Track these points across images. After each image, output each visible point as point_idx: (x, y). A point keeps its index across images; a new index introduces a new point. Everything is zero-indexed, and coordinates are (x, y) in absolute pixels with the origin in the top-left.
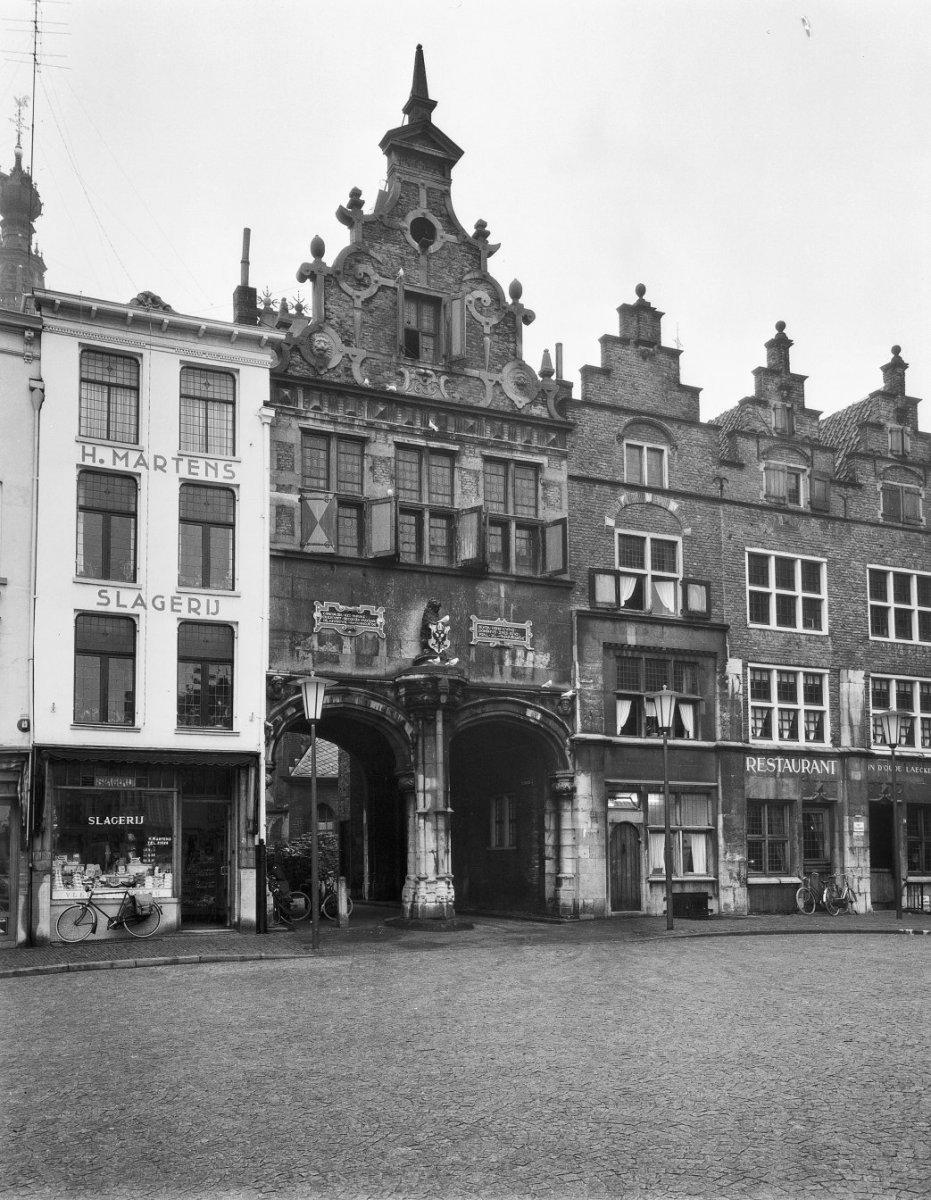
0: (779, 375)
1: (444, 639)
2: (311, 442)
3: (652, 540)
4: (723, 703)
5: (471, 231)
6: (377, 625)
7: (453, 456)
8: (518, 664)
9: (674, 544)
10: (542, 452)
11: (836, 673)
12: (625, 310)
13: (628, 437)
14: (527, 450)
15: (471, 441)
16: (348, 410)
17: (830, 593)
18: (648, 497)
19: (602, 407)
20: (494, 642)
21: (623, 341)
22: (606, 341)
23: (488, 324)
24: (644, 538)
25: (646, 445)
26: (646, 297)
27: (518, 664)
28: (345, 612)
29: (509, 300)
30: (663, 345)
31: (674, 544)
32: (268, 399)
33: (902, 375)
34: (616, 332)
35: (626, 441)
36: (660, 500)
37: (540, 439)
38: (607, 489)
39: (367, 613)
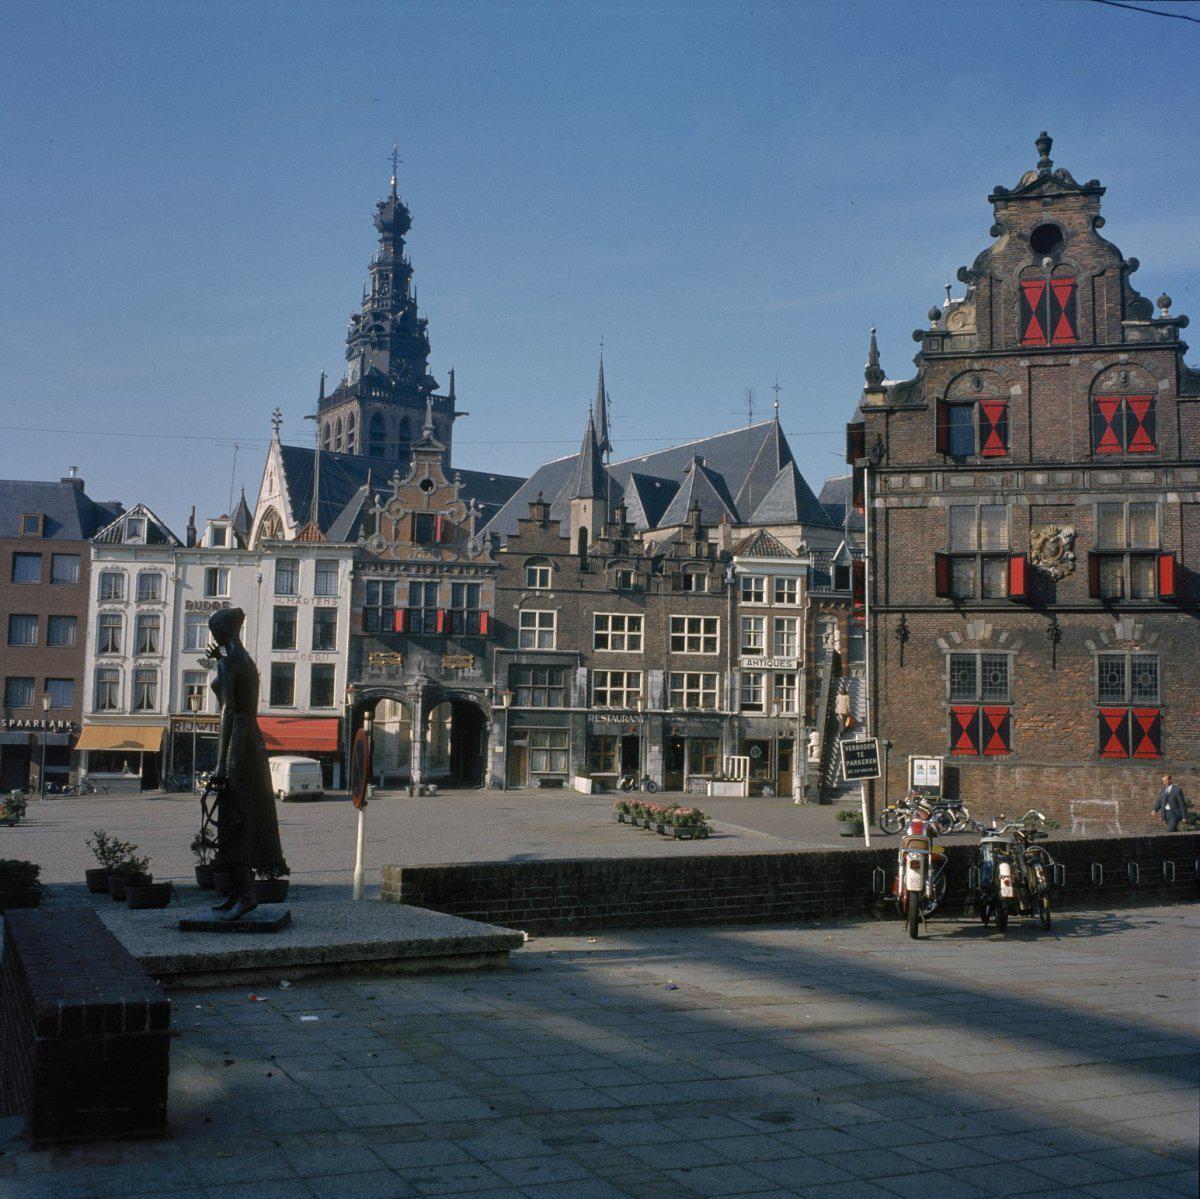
4: (575, 689)
8: (466, 674)
10: (482, 578)
11: (646, 672)
14: (473, 577)
15: (446, 577)
17: (645, 631)
27: (466, 674)
38: (516, 592)
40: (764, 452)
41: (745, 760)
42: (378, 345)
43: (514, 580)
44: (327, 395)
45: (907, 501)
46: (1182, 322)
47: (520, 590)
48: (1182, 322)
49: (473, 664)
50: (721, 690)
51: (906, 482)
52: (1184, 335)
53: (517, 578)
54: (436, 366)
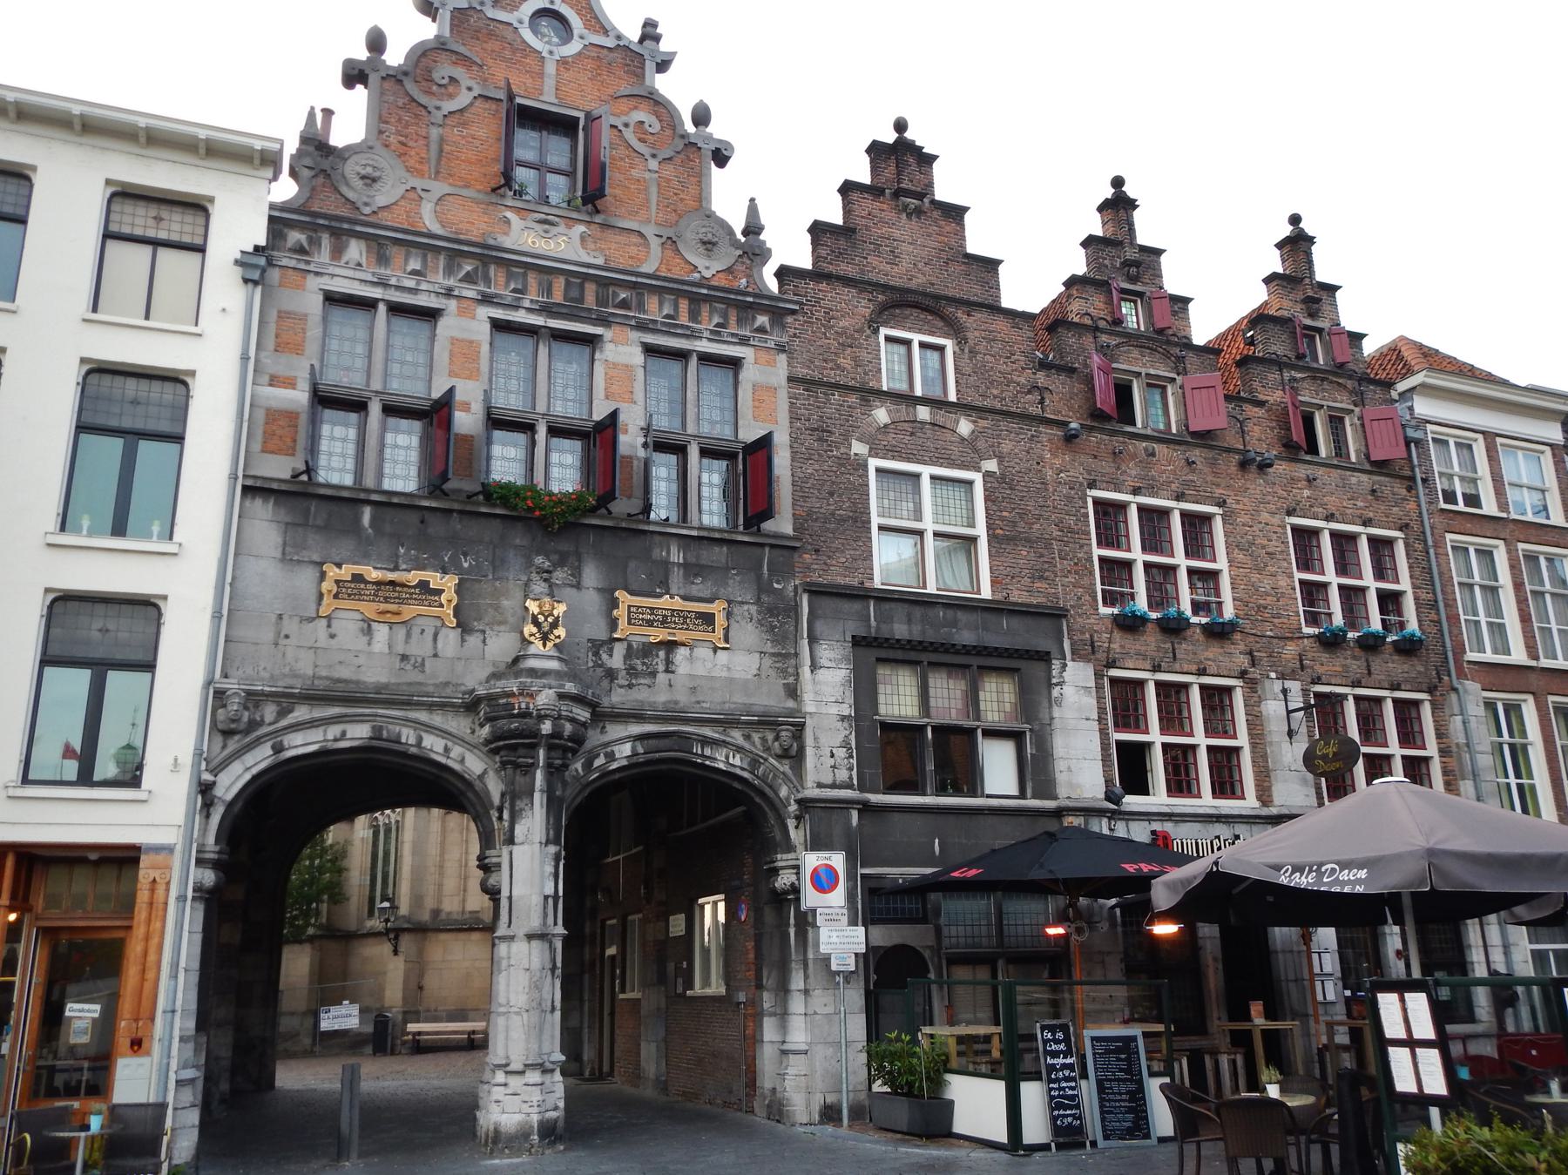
0: (1119, 256)
1: (554, 625)
2: (338, 313)
3: (933, 478)
5: (633, 33)
6: (442, 606)
7: (591, 341)
9: (970, 483)
10: (744, 341)
12: (876, 150)
13: (886, 324)
14: (716, 336)
15: (624, 322)
16: (409, 268)
18: (923, 413)
19: (847, 281)
20: (658, 634)
21: (874, 191)
22: (847, 189)
23: (654, 156)
24: (917, 476)
25: (917, 338)
26: (908, 135)
28: (379, 583)
29: (690, 128)
30: (938, 197)
31: (970, 483)
32: (263, 243)
33: (1309, 255)
34: (864, 177)
35: (883, 331)
36: (942, 417)
37: (739, 322)
39: (423, 585)
41: (706, 982)
43: (845, 362)
49: (727, 630)
50: (1444, 752)
53: (857, 362)
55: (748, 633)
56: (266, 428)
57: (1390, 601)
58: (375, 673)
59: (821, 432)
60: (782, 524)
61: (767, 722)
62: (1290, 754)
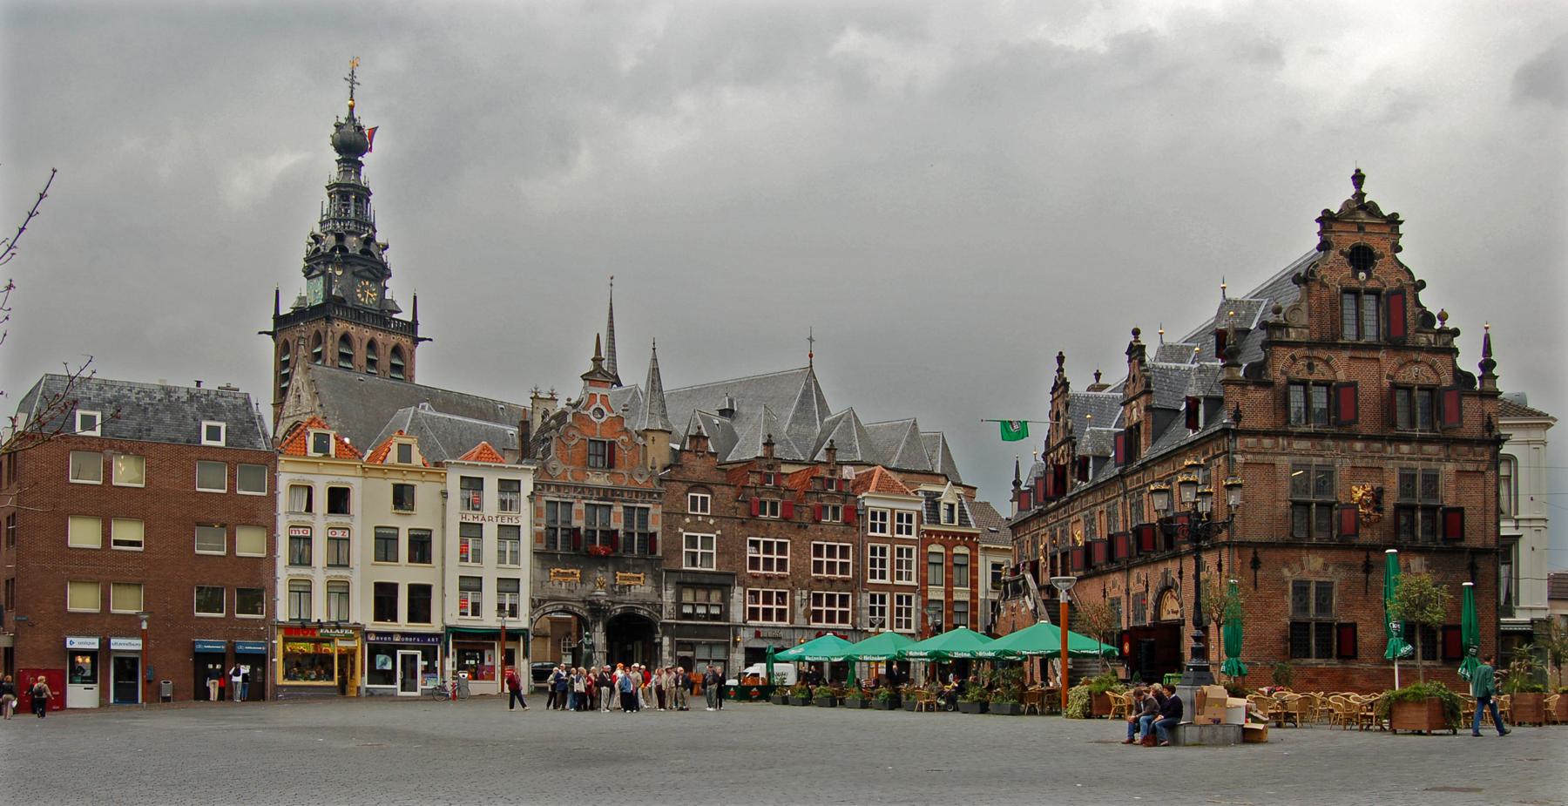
7: (610, 507)
11: (793, 592)
40: (803, 395)
42: (341, 266)
44: (285, 310)
45: (1259, 458)
46: (1456, 332)
47: (685, 515)
48: (1456, 332)
51: (1397, 450)
52: (1457, 342)
54: (397, 291)
55: (649, 581)
56: (537, 537)
57: (844, 566)
58: (563, 595)
59: (670, 527)
60: (659, 553)
61: (654, 604)
62: (800, 611)
